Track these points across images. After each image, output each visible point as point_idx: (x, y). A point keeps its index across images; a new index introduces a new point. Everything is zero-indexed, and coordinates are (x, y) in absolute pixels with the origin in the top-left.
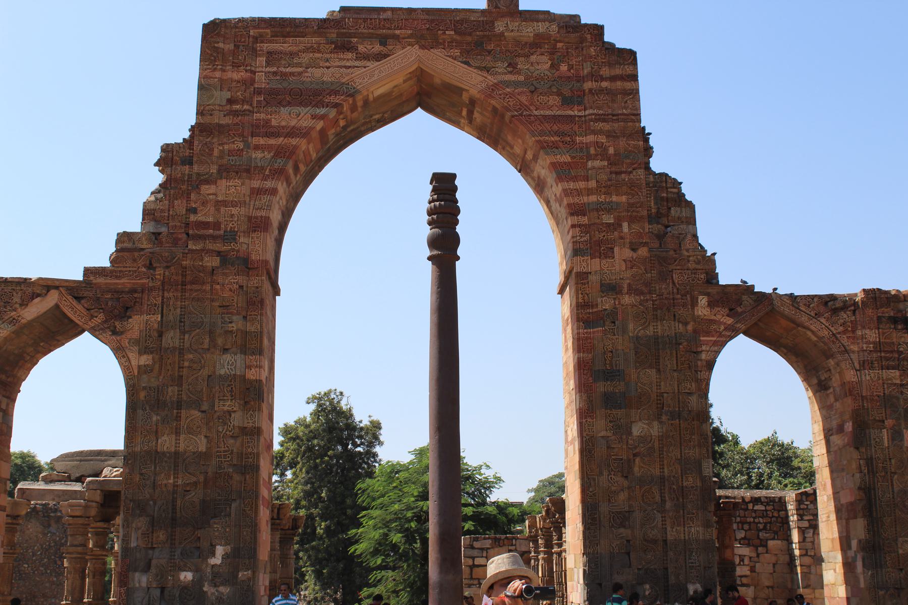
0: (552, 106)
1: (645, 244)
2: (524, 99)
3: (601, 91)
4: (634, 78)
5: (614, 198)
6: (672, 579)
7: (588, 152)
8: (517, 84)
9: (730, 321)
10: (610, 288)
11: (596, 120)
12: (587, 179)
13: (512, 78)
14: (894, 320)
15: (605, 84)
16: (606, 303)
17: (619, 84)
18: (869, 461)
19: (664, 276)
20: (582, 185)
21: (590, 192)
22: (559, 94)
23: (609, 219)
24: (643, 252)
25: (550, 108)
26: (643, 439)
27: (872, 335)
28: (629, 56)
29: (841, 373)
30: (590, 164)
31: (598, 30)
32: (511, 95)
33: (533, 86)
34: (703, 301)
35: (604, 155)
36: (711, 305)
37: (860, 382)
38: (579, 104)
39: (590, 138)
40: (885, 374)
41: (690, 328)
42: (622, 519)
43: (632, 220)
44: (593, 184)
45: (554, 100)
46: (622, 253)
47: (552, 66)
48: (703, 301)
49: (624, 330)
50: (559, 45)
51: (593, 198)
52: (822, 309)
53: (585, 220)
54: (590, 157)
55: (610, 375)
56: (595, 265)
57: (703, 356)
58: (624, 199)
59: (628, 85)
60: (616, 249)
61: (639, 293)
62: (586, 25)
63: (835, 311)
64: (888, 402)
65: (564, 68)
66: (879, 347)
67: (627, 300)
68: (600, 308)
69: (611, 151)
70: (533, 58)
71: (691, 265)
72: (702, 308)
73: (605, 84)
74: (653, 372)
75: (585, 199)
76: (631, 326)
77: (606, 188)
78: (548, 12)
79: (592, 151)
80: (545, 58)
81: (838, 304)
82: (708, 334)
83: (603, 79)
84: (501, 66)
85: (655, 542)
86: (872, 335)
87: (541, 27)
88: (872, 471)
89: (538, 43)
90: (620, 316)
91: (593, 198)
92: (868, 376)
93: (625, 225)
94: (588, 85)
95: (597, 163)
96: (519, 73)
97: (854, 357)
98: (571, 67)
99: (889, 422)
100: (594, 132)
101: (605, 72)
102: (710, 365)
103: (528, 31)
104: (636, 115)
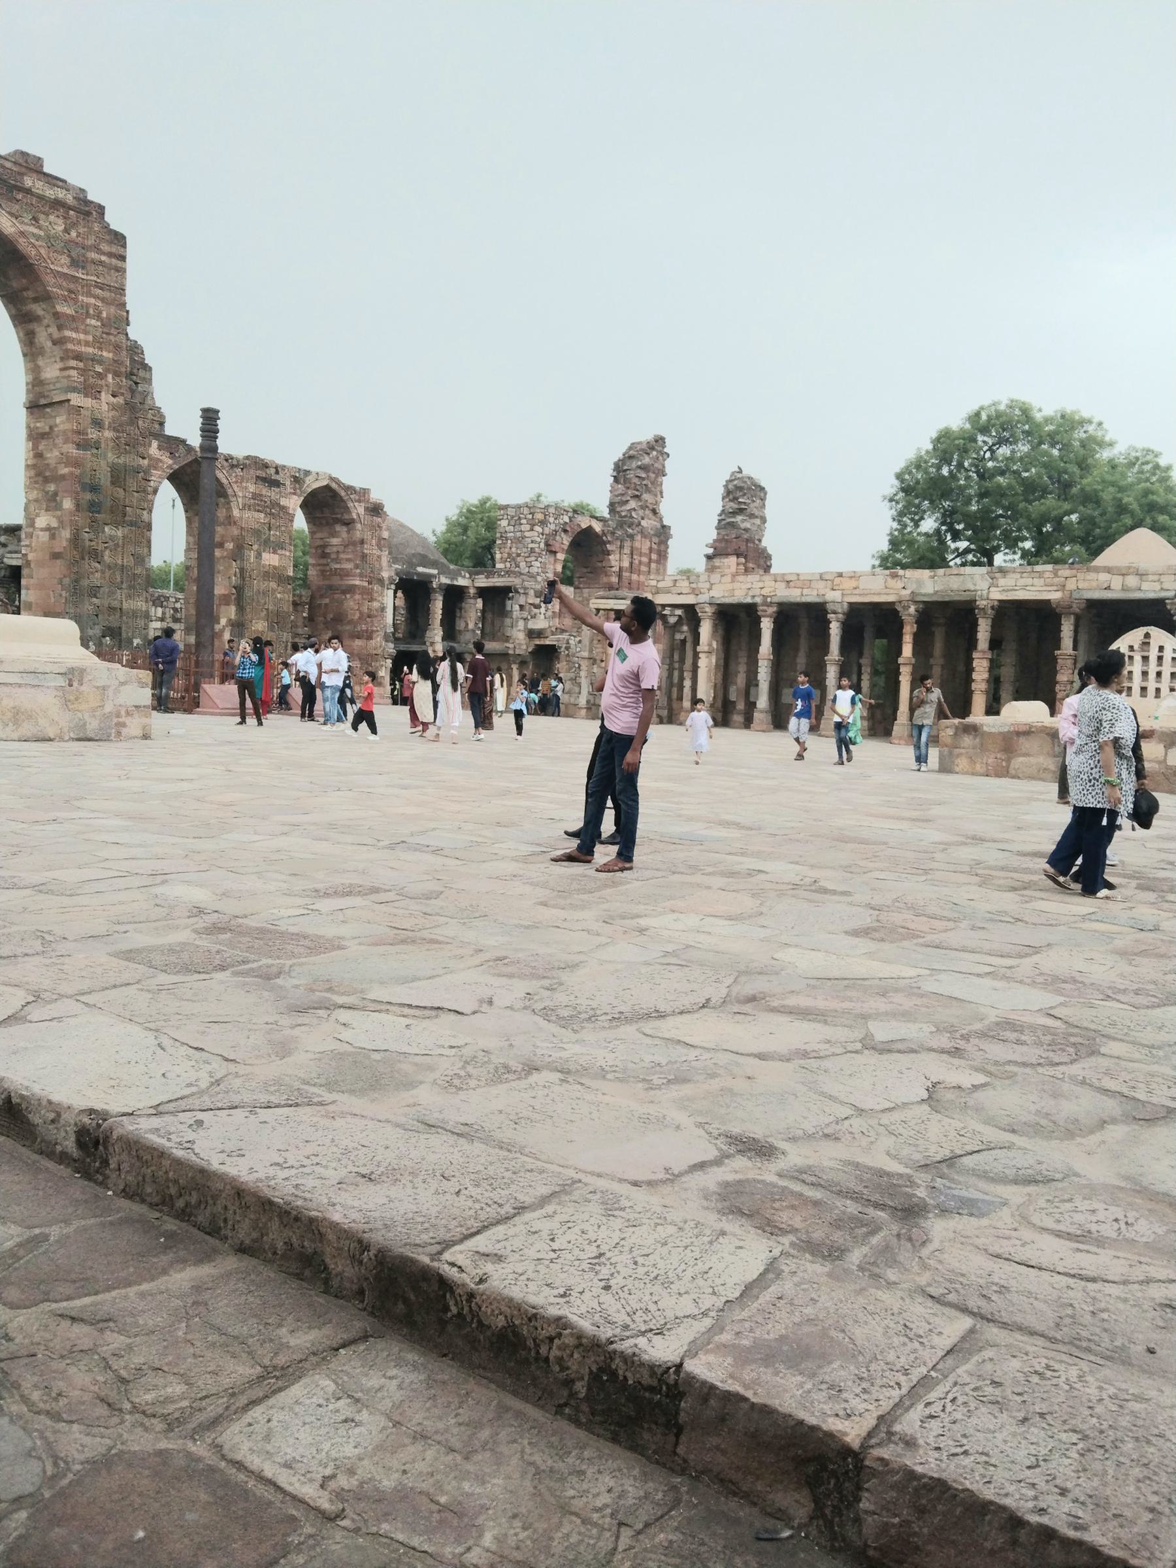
0: (62, 264)
1: (122, 394)
2: (43, 251)
3: (101, 263)
4: (123, 258)
5: (105, 354)
6: (124, 635)
7: (87, 312)
8: (38, 238)
9: (170, 462)
10: (97, 423)
11: (96, 287)
12: (86, 333)
13: (36, 231)
14: (264, 480)
15: (103, 258)
16: (93, 434)
17: (114, 261)
18: (242, 570)
19: (133, 421)
20: (82, 336)
21: (87, 344)
22: (69, 256)
23: (99, 369)
24: (120, 400)
25: (62, 266)
26: (112, 538)
27: (252, 488)
28: (119, 239)
29: (229, 509)
30: (88, 321)
31: (101, 209)
32: (34, 246)
33: (50, 240)
34: (155, 444)
35: (98, 317)
36: (160, 448)
37: (241, 518)
38: (83, 268)
39: (92, 301)
40: (256, 515)
41: (146, 462)
42: (94, 592)
43: (116, 374)
44: (90, 338)
45: (65, 260)
46: (105, 397)
47: (66, 231)
48: (155, 444)
49: (105, 458)
50: (71, 212)
51: (90, 350)
52: (226, 464)
53: (81, 365)
54: (88, 315)
55: (94, 489)
56: (88, 402)
57: (152, 483)
58: (111, 355)
59: (119, 264)
60: (103, 394)
61: (115, 430)
62: (92, 202)
63: (232, 466)
64: (257, 533)
65: (74, 234)
66: (255, 496)
67: (108, 434)
68: (90, 436)
69: (104, 315)
70: (52, 218)
71: (150, 416)
72: (154, 449)
73: (103, 258)
74: (121, 491)
75: (83, 349)
76: (110, 455)
77: (98, 343)
78: (64, 181)
79: (91, 311)
80: (60, 221)
81: (235, 462)
82: (155, 468)
83: (104, 254)
84: (27, 218)
85: (115, 609)
86: (252, 488)
87: (61, 194)
88: (243, 578)
89: (57, 204)
90: (103, 445)
91: (90, 350)
92: (247, 514)
93: (110, 376)
94: (93, 255)
95: (93, 322)
96: (40, 228)
97: (240, 500)
98: (79, 235)
99: (255, 547)
100: (96, 297)
101: (105, 247)
102: (155, 491)
103: (50, 193)
104: (121, 290)
